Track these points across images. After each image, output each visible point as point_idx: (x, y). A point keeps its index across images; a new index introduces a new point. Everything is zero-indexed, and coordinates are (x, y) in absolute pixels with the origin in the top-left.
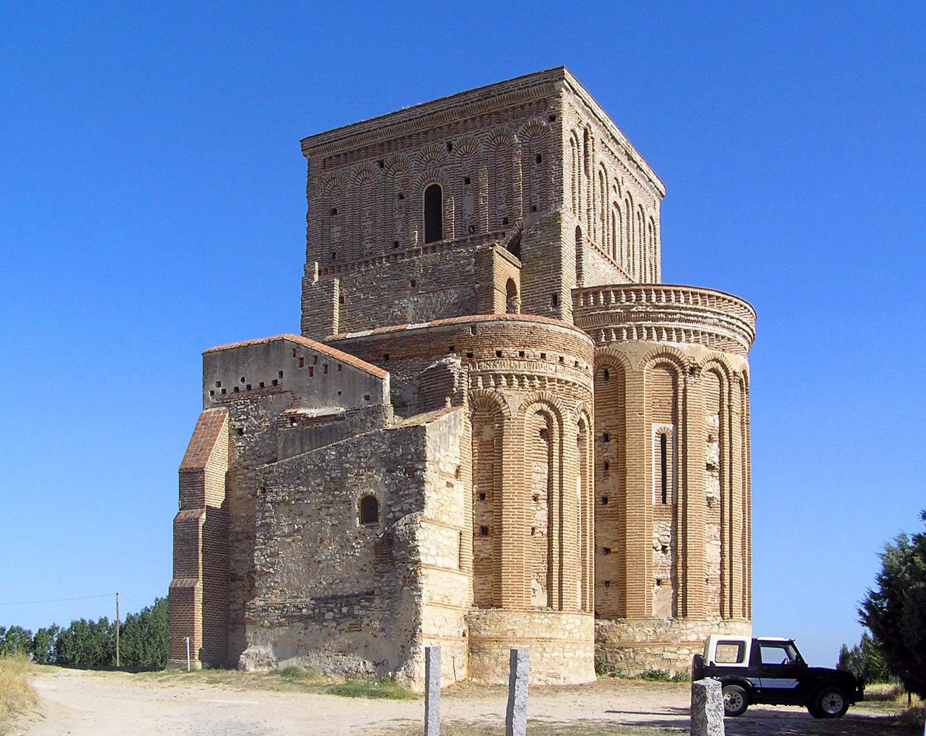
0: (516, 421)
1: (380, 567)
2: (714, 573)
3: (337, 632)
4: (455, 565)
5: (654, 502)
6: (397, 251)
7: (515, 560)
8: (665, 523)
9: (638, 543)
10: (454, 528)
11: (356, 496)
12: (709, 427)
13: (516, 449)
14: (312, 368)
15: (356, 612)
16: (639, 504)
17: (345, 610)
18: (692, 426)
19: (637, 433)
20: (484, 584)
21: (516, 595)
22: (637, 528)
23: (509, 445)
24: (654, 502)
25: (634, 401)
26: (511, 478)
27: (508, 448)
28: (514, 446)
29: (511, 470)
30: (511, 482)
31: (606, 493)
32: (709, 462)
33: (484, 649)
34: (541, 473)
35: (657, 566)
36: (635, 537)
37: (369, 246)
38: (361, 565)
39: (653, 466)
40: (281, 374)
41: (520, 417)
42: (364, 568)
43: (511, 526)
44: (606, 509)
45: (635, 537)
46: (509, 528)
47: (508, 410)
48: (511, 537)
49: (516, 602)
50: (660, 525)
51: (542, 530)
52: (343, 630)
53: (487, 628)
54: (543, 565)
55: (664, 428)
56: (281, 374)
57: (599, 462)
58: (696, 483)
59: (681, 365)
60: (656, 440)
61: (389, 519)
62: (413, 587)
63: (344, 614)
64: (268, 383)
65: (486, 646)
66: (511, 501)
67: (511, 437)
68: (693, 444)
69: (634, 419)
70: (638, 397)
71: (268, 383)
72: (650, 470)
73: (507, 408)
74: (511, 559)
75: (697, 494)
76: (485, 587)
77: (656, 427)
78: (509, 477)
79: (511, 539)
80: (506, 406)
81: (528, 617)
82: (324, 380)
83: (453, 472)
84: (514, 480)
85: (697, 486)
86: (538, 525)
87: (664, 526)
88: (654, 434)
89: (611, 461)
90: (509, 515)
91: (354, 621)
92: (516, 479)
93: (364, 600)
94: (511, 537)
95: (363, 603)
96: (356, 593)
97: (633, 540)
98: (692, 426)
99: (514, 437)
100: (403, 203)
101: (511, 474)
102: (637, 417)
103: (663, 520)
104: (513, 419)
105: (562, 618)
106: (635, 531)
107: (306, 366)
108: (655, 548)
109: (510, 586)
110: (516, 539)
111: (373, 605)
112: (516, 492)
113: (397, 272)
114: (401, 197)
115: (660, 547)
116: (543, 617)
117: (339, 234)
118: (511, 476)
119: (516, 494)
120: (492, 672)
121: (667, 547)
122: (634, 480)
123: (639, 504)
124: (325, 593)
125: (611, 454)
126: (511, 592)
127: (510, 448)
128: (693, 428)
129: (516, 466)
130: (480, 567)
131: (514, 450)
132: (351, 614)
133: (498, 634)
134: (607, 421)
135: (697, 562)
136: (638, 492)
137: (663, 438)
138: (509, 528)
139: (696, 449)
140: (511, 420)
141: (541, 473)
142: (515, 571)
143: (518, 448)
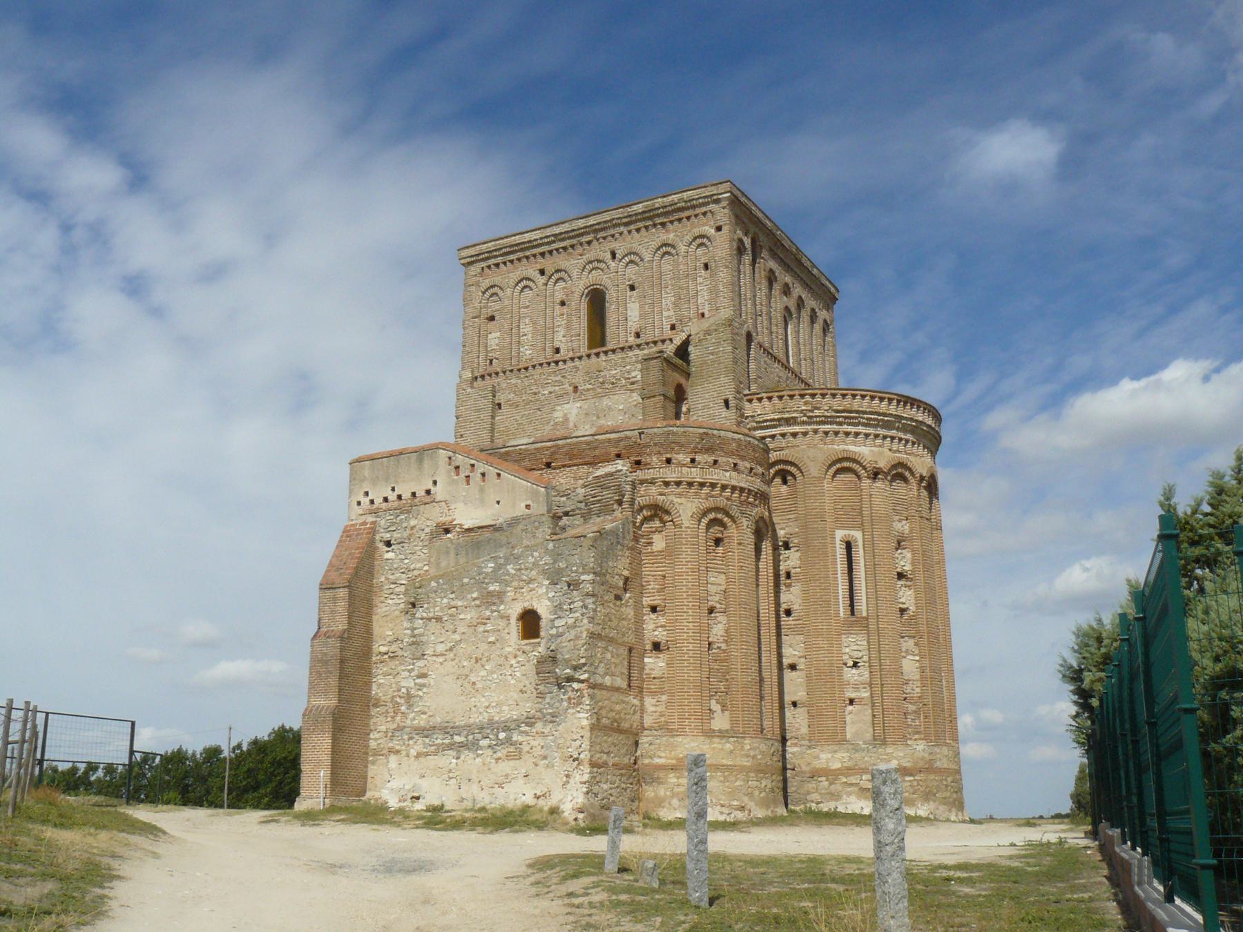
1: (541, 688)
3: (493, 761)
4: (624, 685)
5: (842, 614)
6: (558, 357)
10: (623, 644)
11: (516, 610)
12: (897, 534)
14: (469, 476)
15: (515, 738)
17: (502, 735)
20: (656, 706)
21: (693, 717)
24: (842, 614)
26: (685, 590)
29: (684, 581)
30: (685, 594)
32: (899, 570)
33: (658, 778)
34: (717, 584)
37: (528, 352)
38: (521, 686)
39: (839, 575)
40: (435, 483)
42: (524, 689)
44: (790, 623)
48: (686, 653)
49: (693, 724)
51: (719, 645)
52: (499, 759)
53: (663, 755)
56: (435, 483)
59: (864, 468)
61: (552, 636)
62: (578, 709)
63: (501, 740)
64: (421, 493)
65: (661, 775)
67: (684, 546)
71: (421, 493)
73: (678, 517)
76: (659, 709)
77: (840, 534)
79: (686, 656)
81: (708, 741)
82: (482, 490)
83: (621, 584)
88: (838, 542)
89: (793, 571)
91: (512, 749)
93: (523, 725)
94: (686, 653)
95: (524, 728)
96: (515, 717)
100: (565, 309)
104: (686, 527)
105: (746, 742)
107: (462, 475)
108: (845, 664)
109: (686, 707)
111: (534, 730)
112: (691, 604)
113: (559, 378)
114: (563, 303)
115: (850, 663)
116: (724, 741)
117: (497, 341)
120: (668, 805)
124: (481, 718)
126: (687, 714)
129: (689, 577)
130: (652, 687)
132: (508, 740)
133: (674, 762)
137: (849, 546)
141: (717, 584)
142: (691, 691)
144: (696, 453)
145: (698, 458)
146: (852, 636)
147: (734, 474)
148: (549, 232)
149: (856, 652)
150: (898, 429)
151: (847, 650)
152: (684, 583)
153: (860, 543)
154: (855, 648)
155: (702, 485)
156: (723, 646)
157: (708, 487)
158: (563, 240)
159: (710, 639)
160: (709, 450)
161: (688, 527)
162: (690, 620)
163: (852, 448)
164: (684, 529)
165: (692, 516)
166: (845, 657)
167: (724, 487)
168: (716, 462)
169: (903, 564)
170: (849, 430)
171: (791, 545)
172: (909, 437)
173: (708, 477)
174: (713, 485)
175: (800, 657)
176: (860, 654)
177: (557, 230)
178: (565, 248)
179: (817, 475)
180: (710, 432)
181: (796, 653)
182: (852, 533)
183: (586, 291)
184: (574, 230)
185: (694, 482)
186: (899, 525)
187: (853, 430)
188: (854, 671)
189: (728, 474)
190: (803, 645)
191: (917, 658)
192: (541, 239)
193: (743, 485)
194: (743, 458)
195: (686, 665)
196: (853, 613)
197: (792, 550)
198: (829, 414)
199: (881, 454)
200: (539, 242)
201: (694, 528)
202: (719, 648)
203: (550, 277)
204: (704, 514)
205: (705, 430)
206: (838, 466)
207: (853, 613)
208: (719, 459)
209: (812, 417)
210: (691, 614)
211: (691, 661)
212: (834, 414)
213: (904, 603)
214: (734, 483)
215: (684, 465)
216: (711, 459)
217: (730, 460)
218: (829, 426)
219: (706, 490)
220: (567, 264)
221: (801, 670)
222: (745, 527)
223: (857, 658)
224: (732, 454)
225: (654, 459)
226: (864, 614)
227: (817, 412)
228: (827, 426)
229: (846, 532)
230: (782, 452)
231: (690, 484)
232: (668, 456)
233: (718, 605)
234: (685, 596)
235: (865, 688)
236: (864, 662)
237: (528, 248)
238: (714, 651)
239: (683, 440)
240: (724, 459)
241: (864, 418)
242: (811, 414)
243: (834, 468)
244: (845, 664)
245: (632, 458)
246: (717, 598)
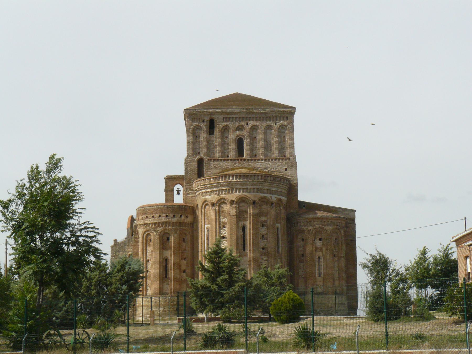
145: (143, 217)
150: (221, 187)
160: (145, 214)
163: (207, 197)
167: (150, 224)
168: (147, 217)
172: (227, 188)
180: (145, 208)
186: (224, 220)
189: (151, 220)
193: (156, 222)
194: (155, 213)
199: (214, 197)
204: (145, 233)
208: (148, 216)
214: (152, 222)
216: (145, 216)
218: (203, 190)
228: (202, 191)
231: (142, 224)
233: (150, 259)
240: (149, 215)
246: (149, 257)
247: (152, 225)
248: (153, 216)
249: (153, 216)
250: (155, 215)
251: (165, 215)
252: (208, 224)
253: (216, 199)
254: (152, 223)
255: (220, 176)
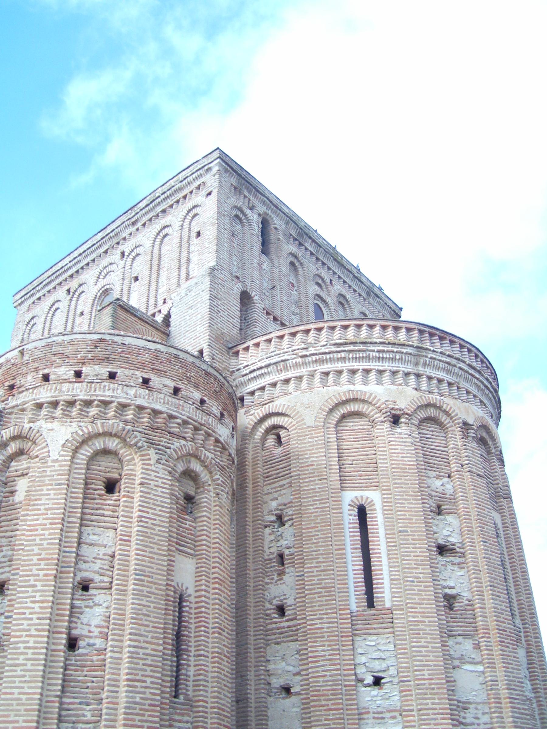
0: (57, 464)
2: (477, 721)
7: (24, 697)
8: (374, 638)
9: (328, 673)
13: (50, 506)
16: (326, 609)
18: (403, 489)
19: (318, 506)
22: (325, 648)
23: (40, 499)
25: (310, 463)
26: (36, 551)
27: (37, 505)
28: (47, 502)
29: (38, 538)
31: (281, 600)
32: (441, 542)
35: (368, 713)
36: (322, 663)
41: (63, 458)
43: (24, 633)
45: (322, 663)
46: (21, 636)
47: (46, 450)
48: (22, 654)
50: (368, 643)
54: (88, 708)
55: (362, 497)
57: (271, 556)
58: (417, 571)
60: (351, 515)
66: (30, 589)
67: (45, 488)
68: (407, 514)
69: (312, 487)
70: (317, 457)
72: (343, 556)
73: (45, 447)
74: (16, 696)
75: (422, 588)
78: (33, 550)
79: (22, 657)
80: (44, 444)
84: (40, 554)
85: (421, 575)
86: (85, 633)
87: (373, 643)
88: (346, 507)
89: (287, 552)
90: (24, 613)
92: (44, 552)
94: (22, 654)
97: (319, 669)
98: (403, 489)
99: (50, 487)
101: (36, 545)
102: (316, 485)
103: (370, 634)
104: (53, 461)
106: (323, 653)
110: (30, 656)
112: (41, 573)
115: (369, 680)
118: (36, 548)
119: (41, 577)
121: (383, 678)
122: (315, 573)
123: (326, 609)
125: (286, 542)
127: (40, 505)
128: (404, 492)
129: (47, 532)
131: (47, 506)
134: (279, 498)
135: (437, 701)
136: (323, 590)
138: (21, 636)
139: (414, 521)
140: (50, 464)
143: (53, 504)
144: (83, 363)
145: (85, 370)
146: (370, 638)
147: (144, 392)
148: (76, 254)
149: (377, 662)
151: (363, 659)
152: (38, 541)
153: (378, 505)
154: (376, 655)
155: (88, 403)
156: (99, 643)
157: (98, 406)
158: (86, 257)
159: (74, 632)
161: (57, 461)
162: (38, 599)
164: (50, 464)
165: (64, 445)
166: (361, 670)
167: (123, 406)
168: (112, 376)
169: (446, 533)
170: (355, 367)
171: (286, 519)
173: (98, 392)
174: (106, 404)
175: (295, 675)
176: (384, 665)
177: (81, 250)
178: (88, 264)
179: (312, 424)
181: (291, 668)
182: (367, 494)
183: (99, 294)
184: (94, 244)
185: (75, 401)
186: (438, 483)
187: (361, 368)
188: (375, 691)
189: (132, 392)
190: (297, 656)
191: (480, 668)
192: (70, 262)
193: (158, 407)
195: (19, 673)
196: (371, 604)
197: (287, 525)
198: (327, 351)
200: (70, 265)
201: (65, 461)
202: (89, 645)
203: (74, 293)
205: (99, 336)
206: (343, 410)
207: (371, 604)
208: (119, 371)
209: (306, 356)
210: (39, 588)
211: (29, 667)
212: (333, 349)
213: (452, 588)
214: (139, 402)
215: (66, 381)
216: (104, 371)
217: (137, 372)
218: (329, 365)
219: (93, 411)
220: (87, 276)
221: (298, 694)
222: (152, 462)
223: (379, 671)
224: (142, 366)
225: (29, 378)
226: (388, 605)
227: (312, 350)
228: (326, 366)
229: (358, 494)
230: (271, 404)
231: (71, 403)
232: (46, 371)
233: (97, 578)
234: (35, 561)
235: (394, 717)
236: (391, 676)
237: (60, 275)
238: (81, 651)
239: (68, 350)
241: (374, 351)
242: (304, 353)
243: (337, 415)
244: (362, 681)
245: (7, 384)
246: (96, 567)
247: (137, 417)
248: (146, 382)
249: (146, 382)
250: (156, 381)
251: (197, 395)
252: (354, 488)
253: (409, 399)
254: (141, 408)
255: (427, 329)
